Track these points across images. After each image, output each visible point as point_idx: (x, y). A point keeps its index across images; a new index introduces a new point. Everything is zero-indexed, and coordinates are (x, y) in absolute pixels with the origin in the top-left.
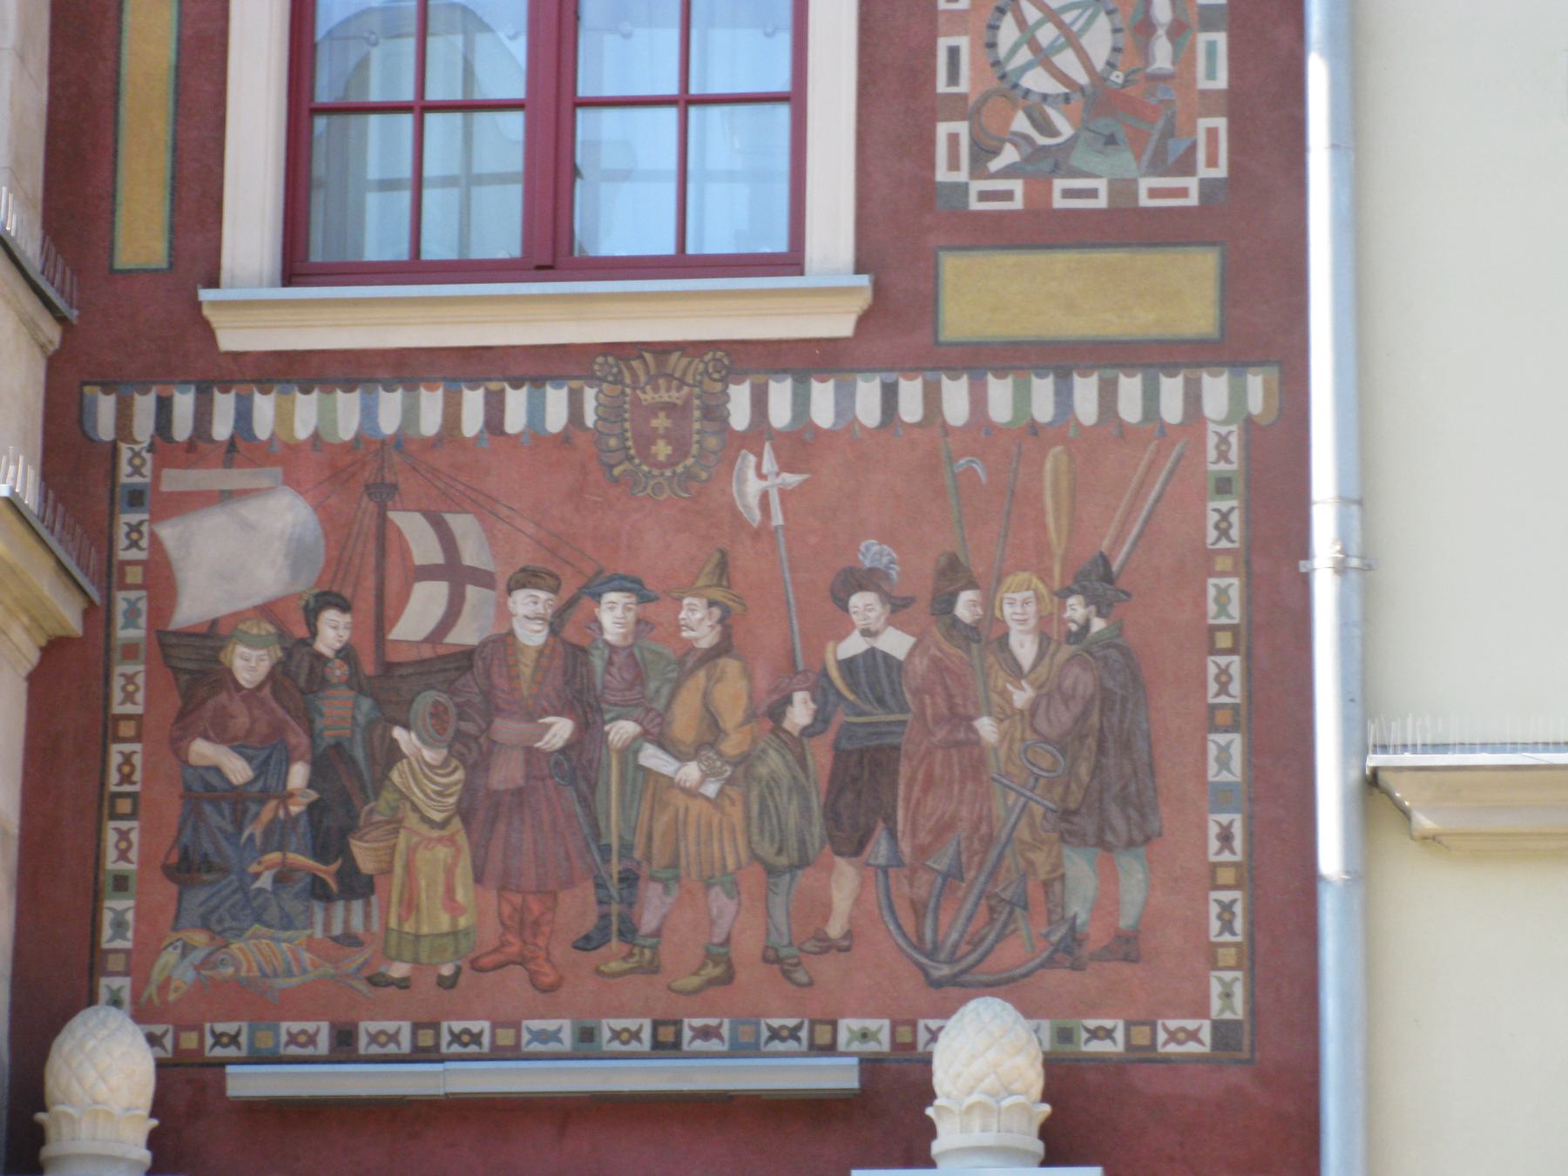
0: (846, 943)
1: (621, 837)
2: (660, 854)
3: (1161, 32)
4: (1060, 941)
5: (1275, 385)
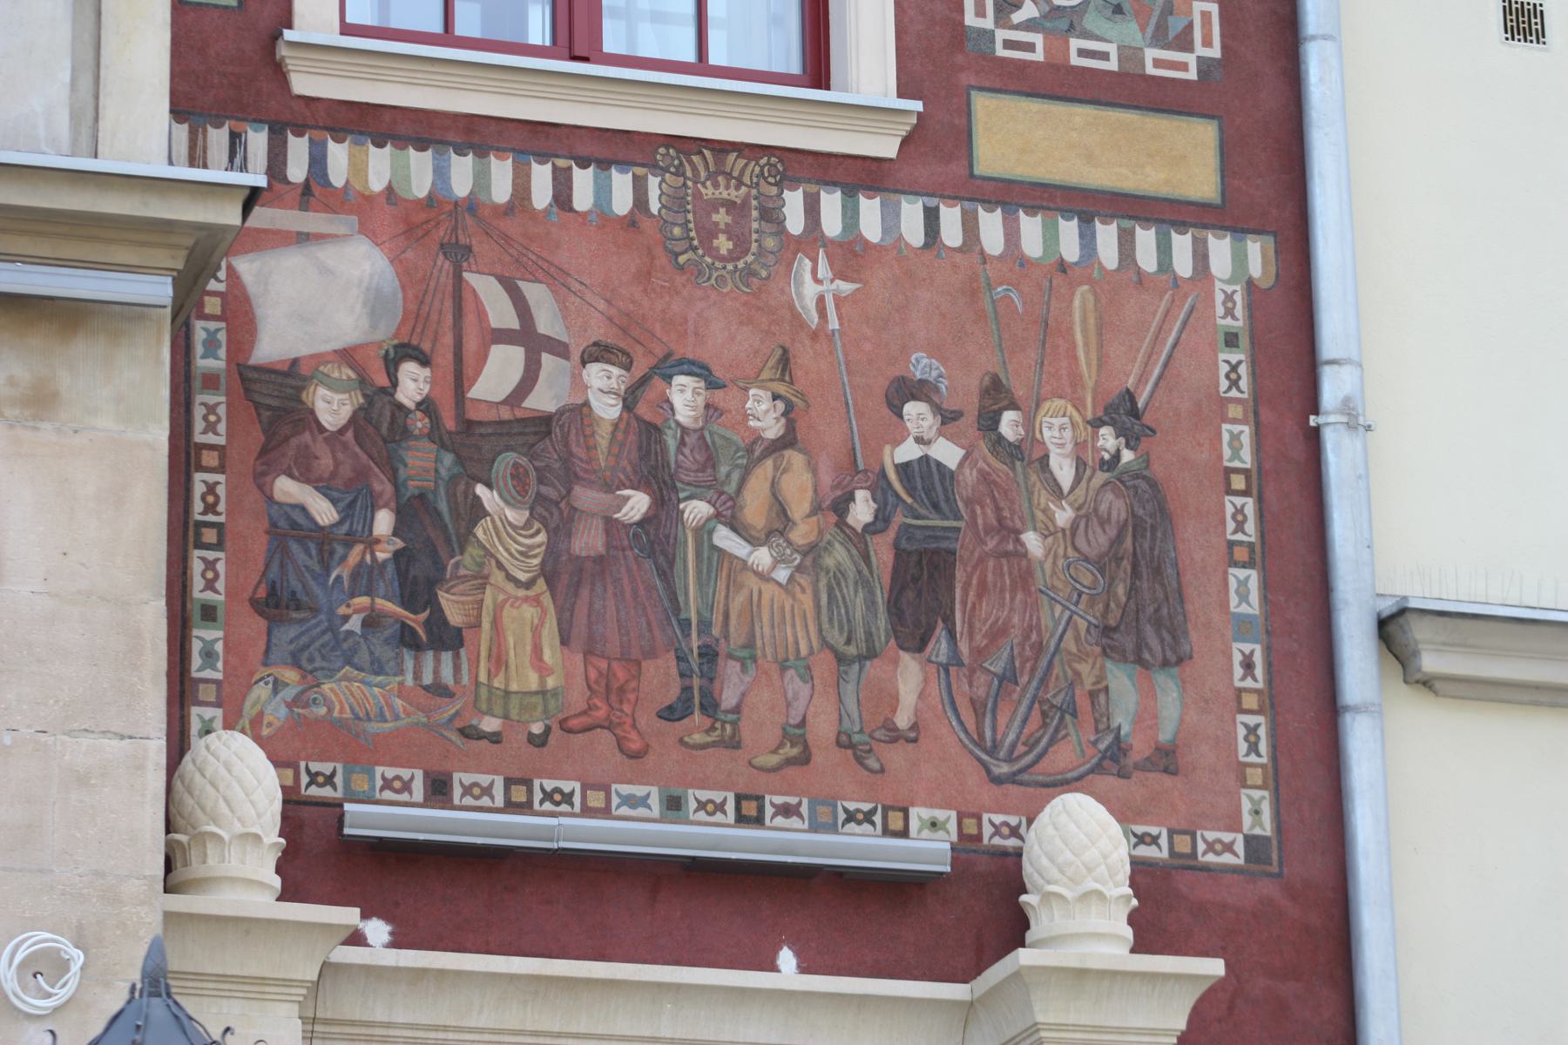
0: (913, 735)
1: (698, 612)
2: (737, 635)
4: (1107, 750)
5: (1272, 253)
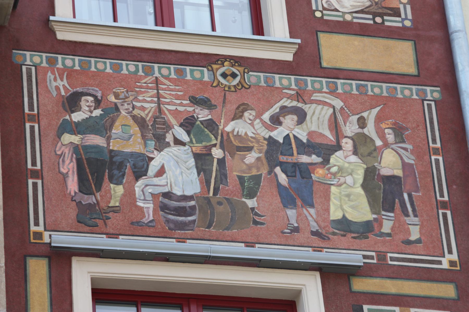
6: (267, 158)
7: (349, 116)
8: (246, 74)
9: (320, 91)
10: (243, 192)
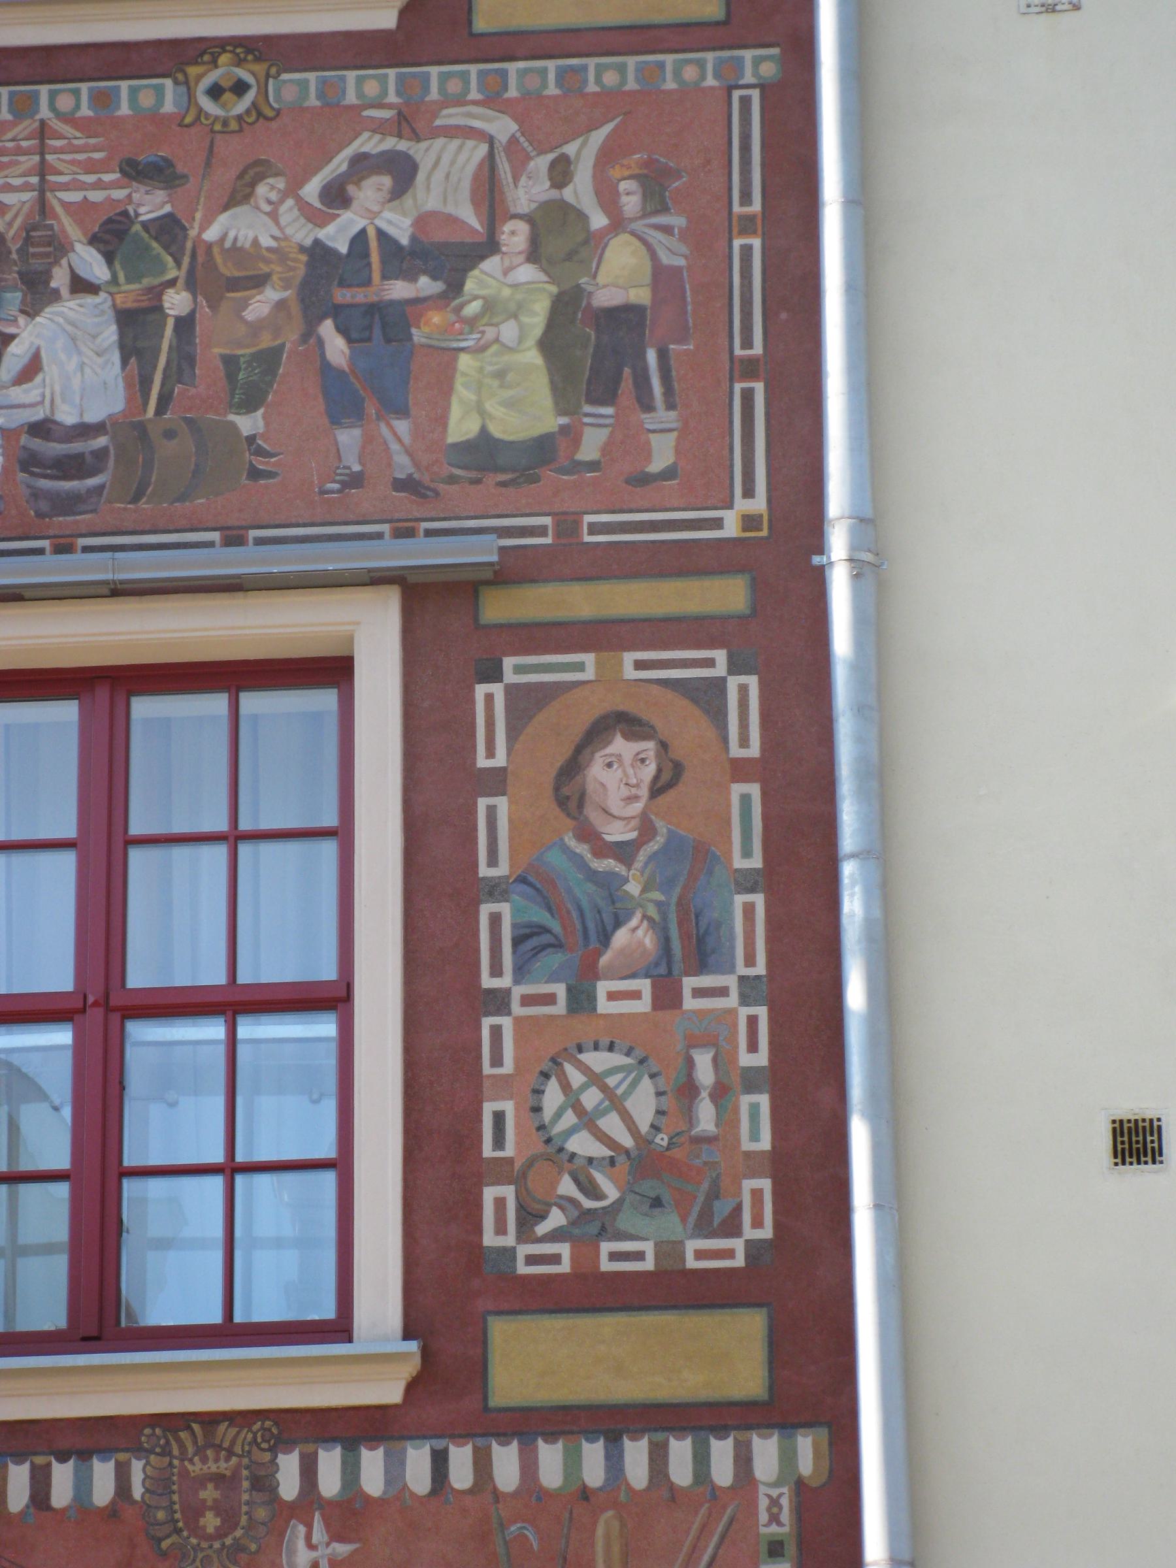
3: (704, 1094)
6: (302, 301)
7: (529, 158)
8: (271, 81)
9: (460, 101)
10: (233, 397)
